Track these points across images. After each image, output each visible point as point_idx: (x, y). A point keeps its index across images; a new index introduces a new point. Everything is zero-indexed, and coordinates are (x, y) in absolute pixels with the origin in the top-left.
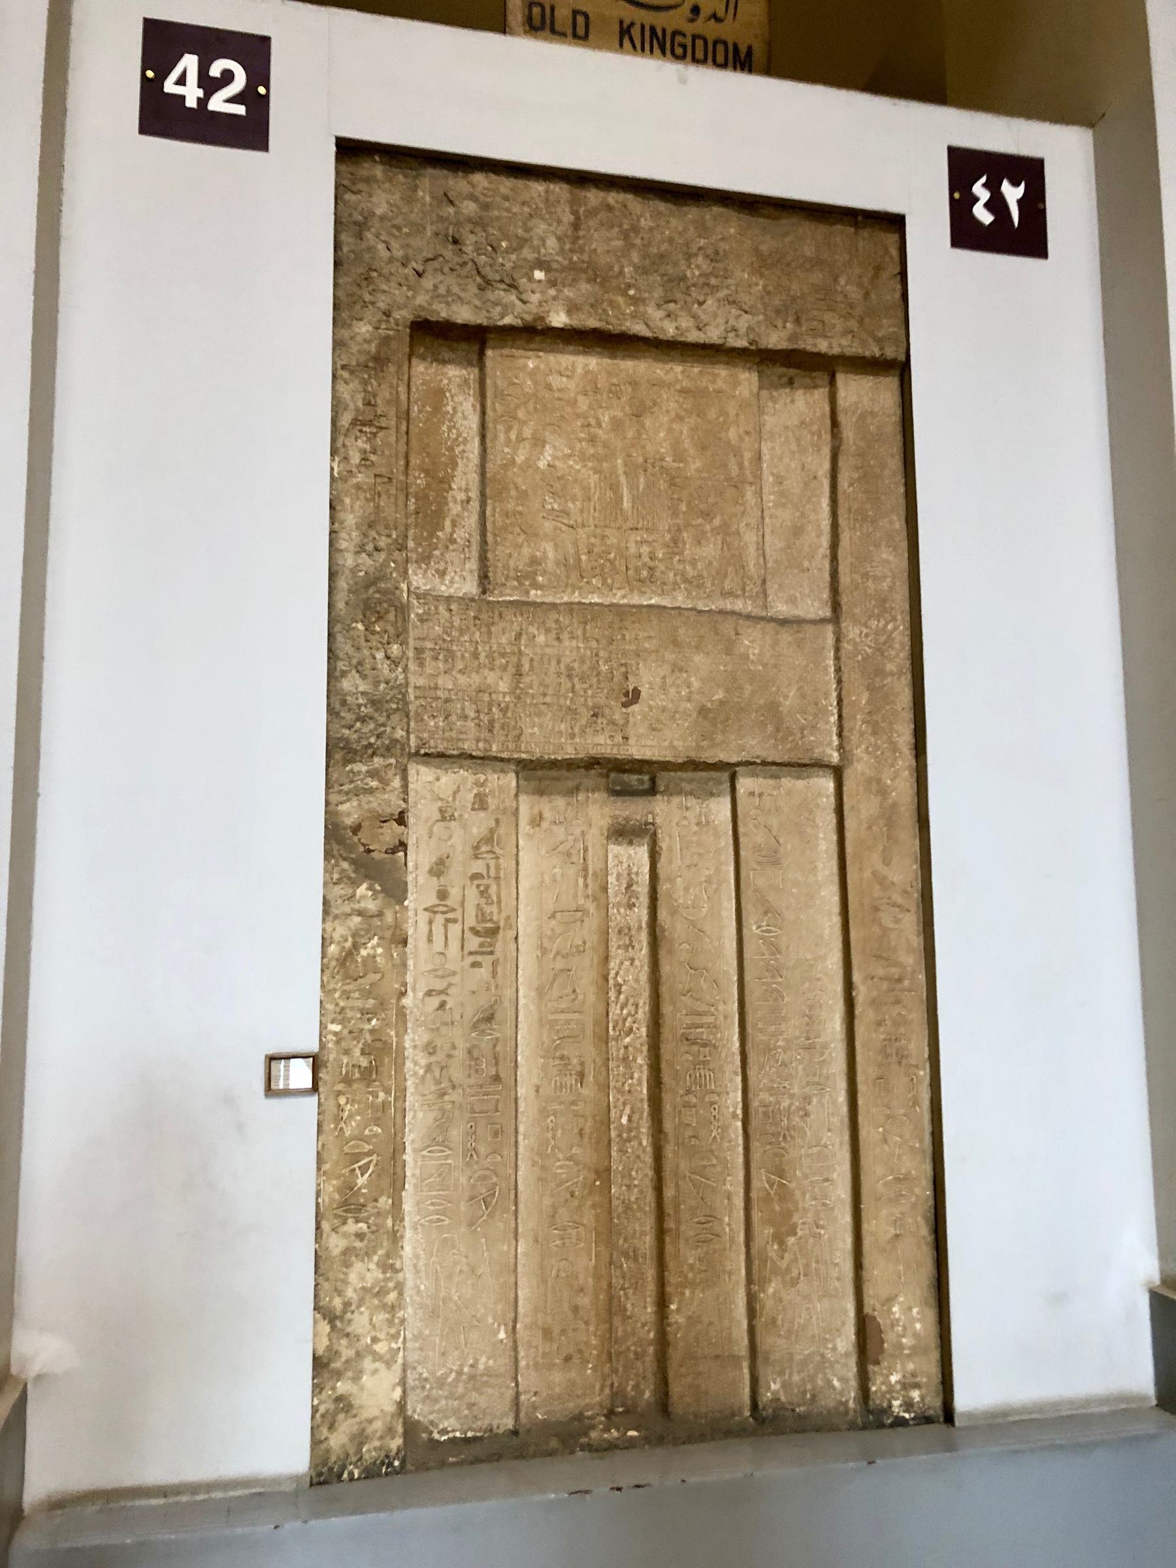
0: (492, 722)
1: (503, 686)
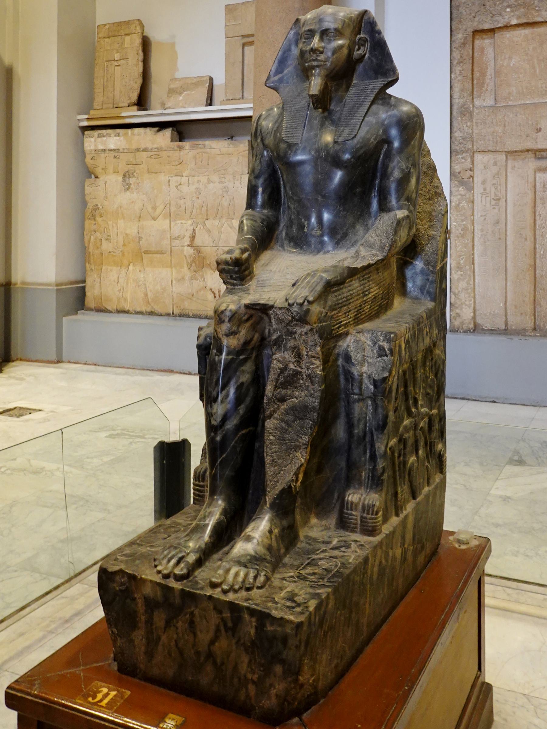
0: (497, 141)
1: (500, 131)
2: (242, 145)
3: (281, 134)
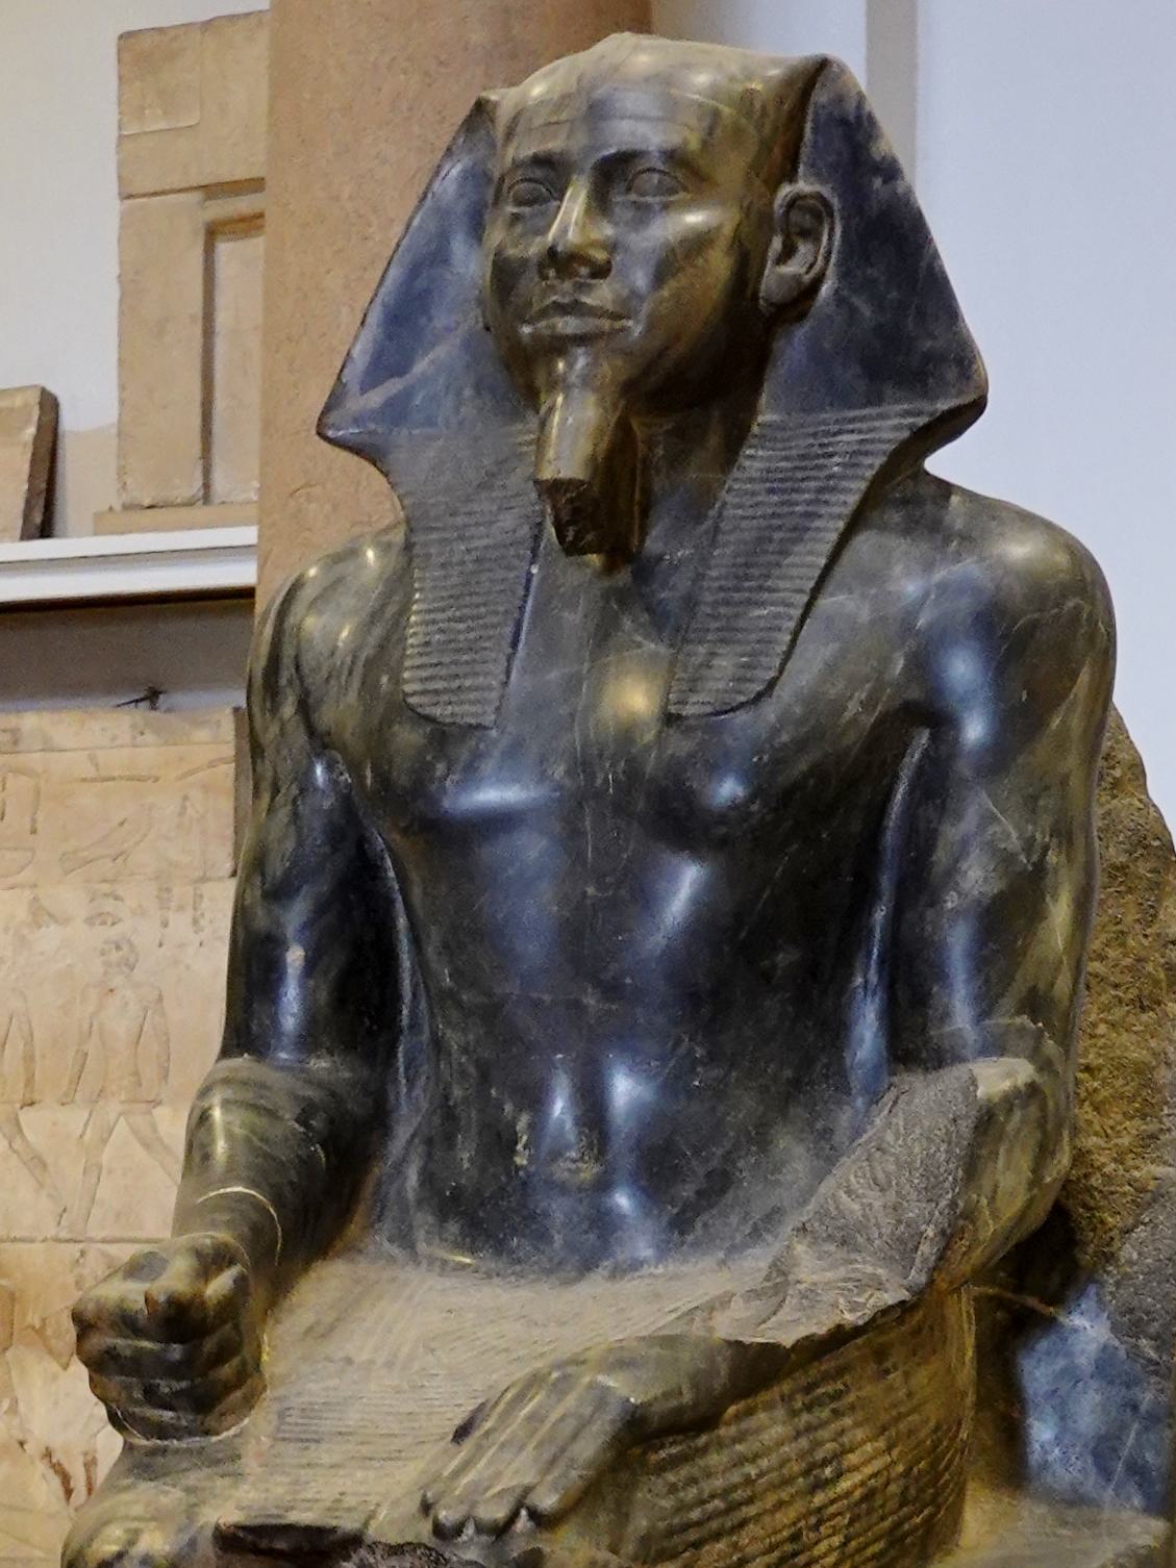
2: (202, 735)
3: (396, 680)
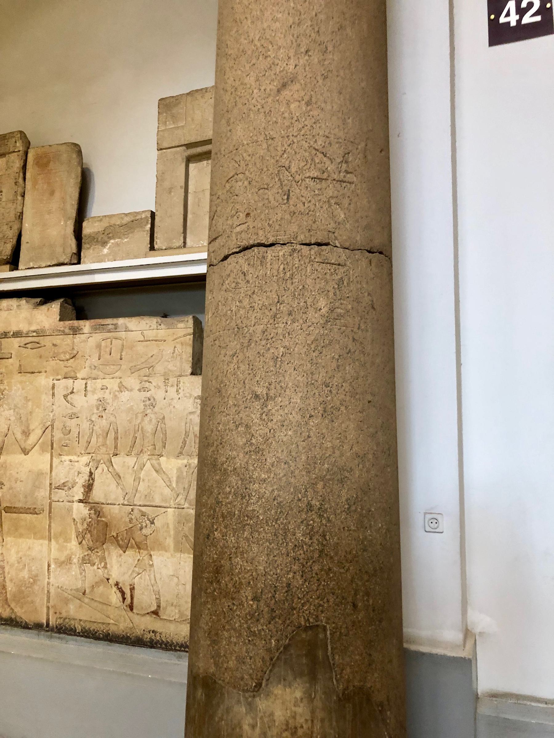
2: (181, 325)
